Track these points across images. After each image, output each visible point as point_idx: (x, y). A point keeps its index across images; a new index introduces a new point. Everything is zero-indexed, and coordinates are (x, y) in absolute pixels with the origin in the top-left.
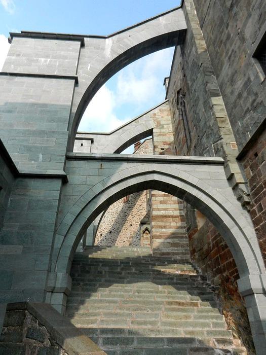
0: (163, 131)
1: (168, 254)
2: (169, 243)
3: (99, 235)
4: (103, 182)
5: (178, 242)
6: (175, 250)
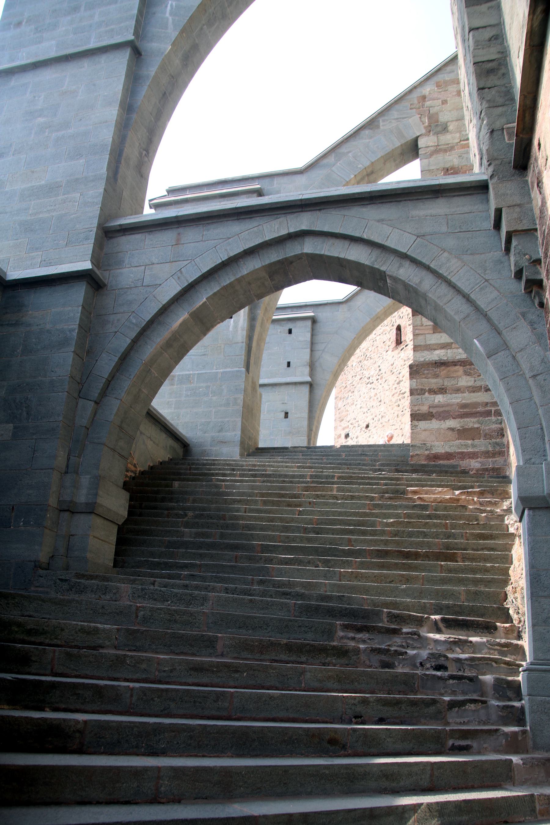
0: (446, 139)
1: (449, 456)
3: (343, 436)
4: (179, 275)
5: (476, 426)
6: (466, 446)
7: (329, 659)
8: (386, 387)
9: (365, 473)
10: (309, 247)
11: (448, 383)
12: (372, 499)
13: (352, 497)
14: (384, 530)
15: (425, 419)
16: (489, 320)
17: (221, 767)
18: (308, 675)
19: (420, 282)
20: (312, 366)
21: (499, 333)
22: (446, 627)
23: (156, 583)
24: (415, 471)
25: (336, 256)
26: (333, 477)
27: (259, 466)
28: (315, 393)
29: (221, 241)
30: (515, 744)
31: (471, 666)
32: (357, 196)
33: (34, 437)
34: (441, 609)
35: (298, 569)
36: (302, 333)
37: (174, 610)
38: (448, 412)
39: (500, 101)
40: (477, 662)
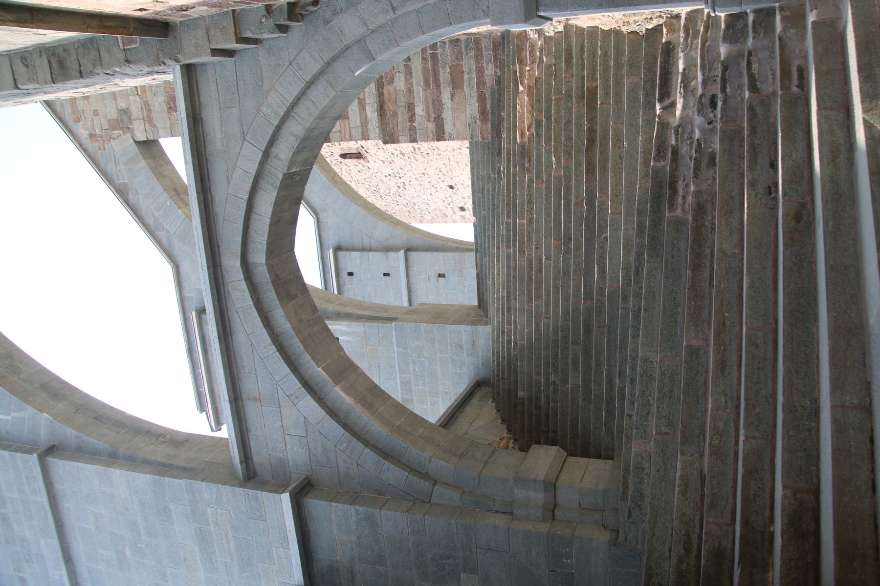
0: (136, 110)
1: (482, 99)
2: (453, 96)
3: (463, 213)
4: (292, 398)
5: (448, 70)
6: (470, 79)
7: (707, 223)
8: (409, 167)
9: (503, 190)
10: (259, 257)
11: (402, 101)
12: (531, 180)
13: (530, 202)
14: (565, 167)
15: (443, 125)
16: (334, 60)
17: (829, 338)
18: (725, 246)
19: (295, 135)
20: (387, 249)
21: (348, 48)
22: (669, 97)
23: (630, 413)
24: (499, 135)
25: (268, 228)
26: (508, 224)
27: (498, 304)
28: (417, 245)
29: (255, 354)
30: (796, 19)
31: (710, 69)
32: (203, 207)
33: (474, 550)
34: (649, 103)
35: (610, 259)
36: (352, 261)
37: (659, 393)
38: (433, 101)
39: (93, 53)
40: (706, 62)
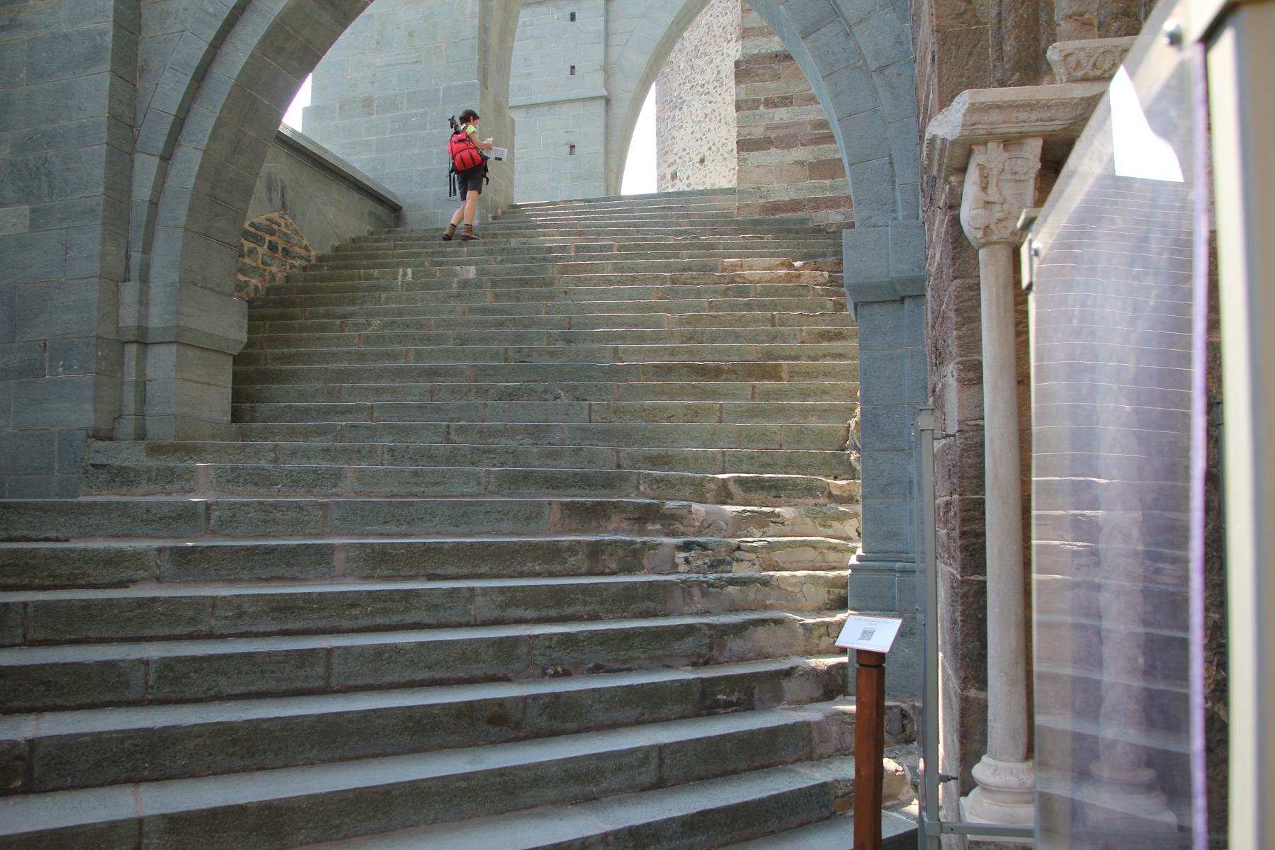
1: (795, 205)
2: (801, 163)
3: (669, 177)
6: (823, 189)
9: (661, 239)
15: (759, 149)
18: (480, 600)
20: (607, 69)
26: (610, 248)
33: (64, 225)
34: (740, 461)
37: (271, 505)
38: (794, 135)
